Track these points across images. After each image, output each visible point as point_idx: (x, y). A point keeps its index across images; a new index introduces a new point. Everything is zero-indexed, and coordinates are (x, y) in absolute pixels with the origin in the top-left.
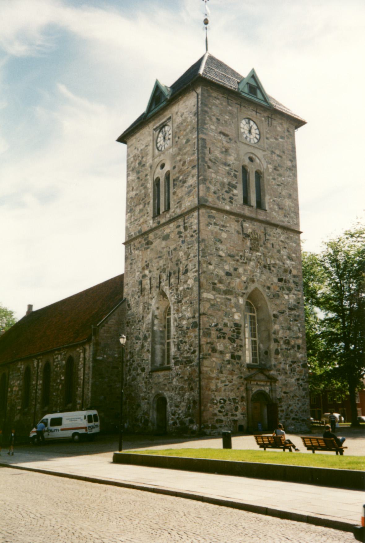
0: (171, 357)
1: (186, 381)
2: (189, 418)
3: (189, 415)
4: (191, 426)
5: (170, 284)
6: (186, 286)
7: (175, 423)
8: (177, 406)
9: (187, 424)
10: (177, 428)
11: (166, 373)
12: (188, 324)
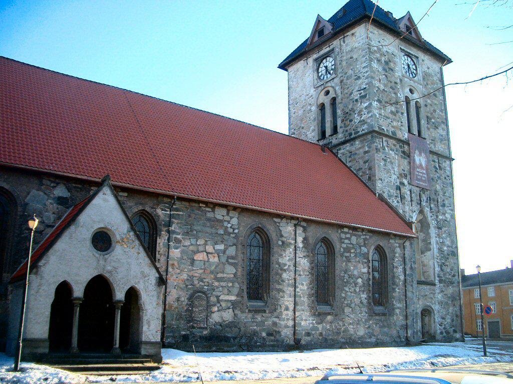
0: (436, 275)
1: (449, 297)
2: (453, 328)
3: (453, 326)
4: (455, 335)
5: (431, 209)
6: (444, 218)
7: (441, 333)
8: (443, 318)
9: (452, 333)
10: (444, 337)
11: (432, 287)
12: (448, 250)
